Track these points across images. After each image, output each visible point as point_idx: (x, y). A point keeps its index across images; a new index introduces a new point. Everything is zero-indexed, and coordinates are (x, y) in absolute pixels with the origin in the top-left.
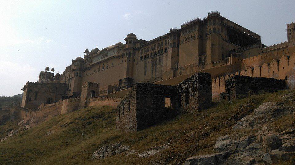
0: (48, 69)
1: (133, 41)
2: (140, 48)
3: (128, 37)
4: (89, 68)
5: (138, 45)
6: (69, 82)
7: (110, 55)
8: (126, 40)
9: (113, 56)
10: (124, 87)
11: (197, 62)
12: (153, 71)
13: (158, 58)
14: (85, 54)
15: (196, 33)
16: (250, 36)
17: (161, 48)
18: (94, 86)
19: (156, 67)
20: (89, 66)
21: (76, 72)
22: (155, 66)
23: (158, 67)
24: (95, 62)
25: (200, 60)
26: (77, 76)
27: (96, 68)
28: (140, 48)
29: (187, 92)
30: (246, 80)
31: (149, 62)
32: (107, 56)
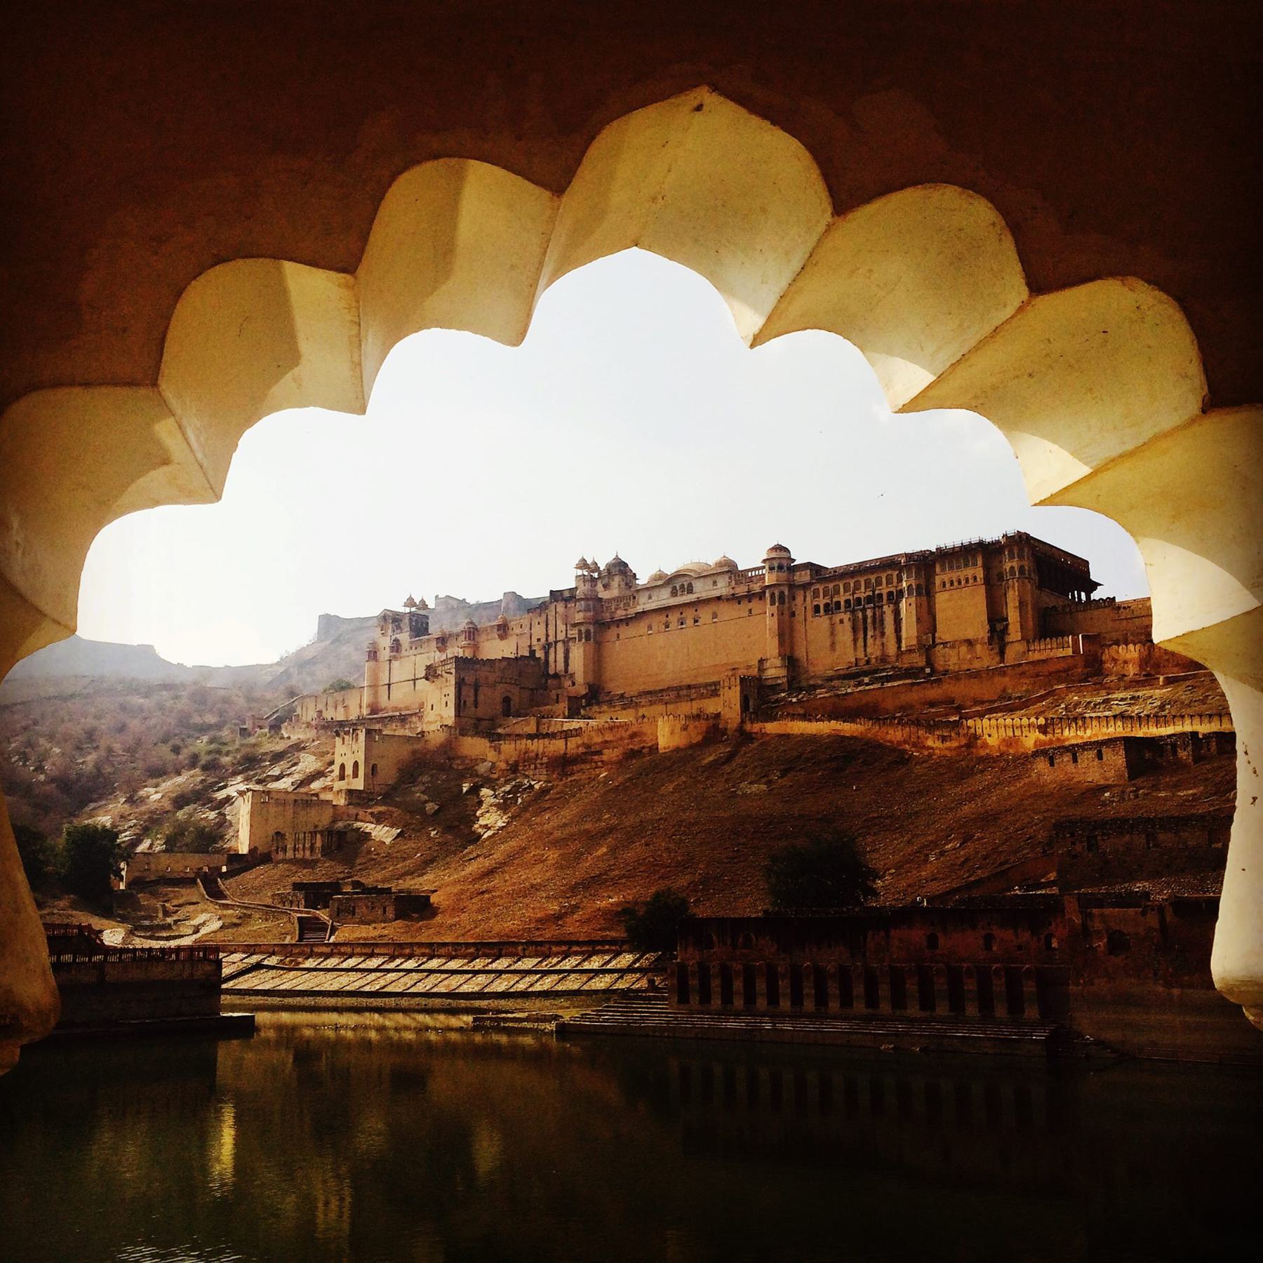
0: (410, 602)
2: (810, 584)
4: (627, 621)
5: (804, 577)
7: (702, 590)
8: (764, 561)
9: (716, 593)
12: (855, 641)
14: (580, 572)
15: (980, 573)
20: (620, 614)
23: (870, 633)
24: (644, 604)
25: (992, 630)
26: (588, 638)
27: (658, 621)
28: (810, 584)
29: (1174, 746)
31: (842, 621)
32: (690, 591)
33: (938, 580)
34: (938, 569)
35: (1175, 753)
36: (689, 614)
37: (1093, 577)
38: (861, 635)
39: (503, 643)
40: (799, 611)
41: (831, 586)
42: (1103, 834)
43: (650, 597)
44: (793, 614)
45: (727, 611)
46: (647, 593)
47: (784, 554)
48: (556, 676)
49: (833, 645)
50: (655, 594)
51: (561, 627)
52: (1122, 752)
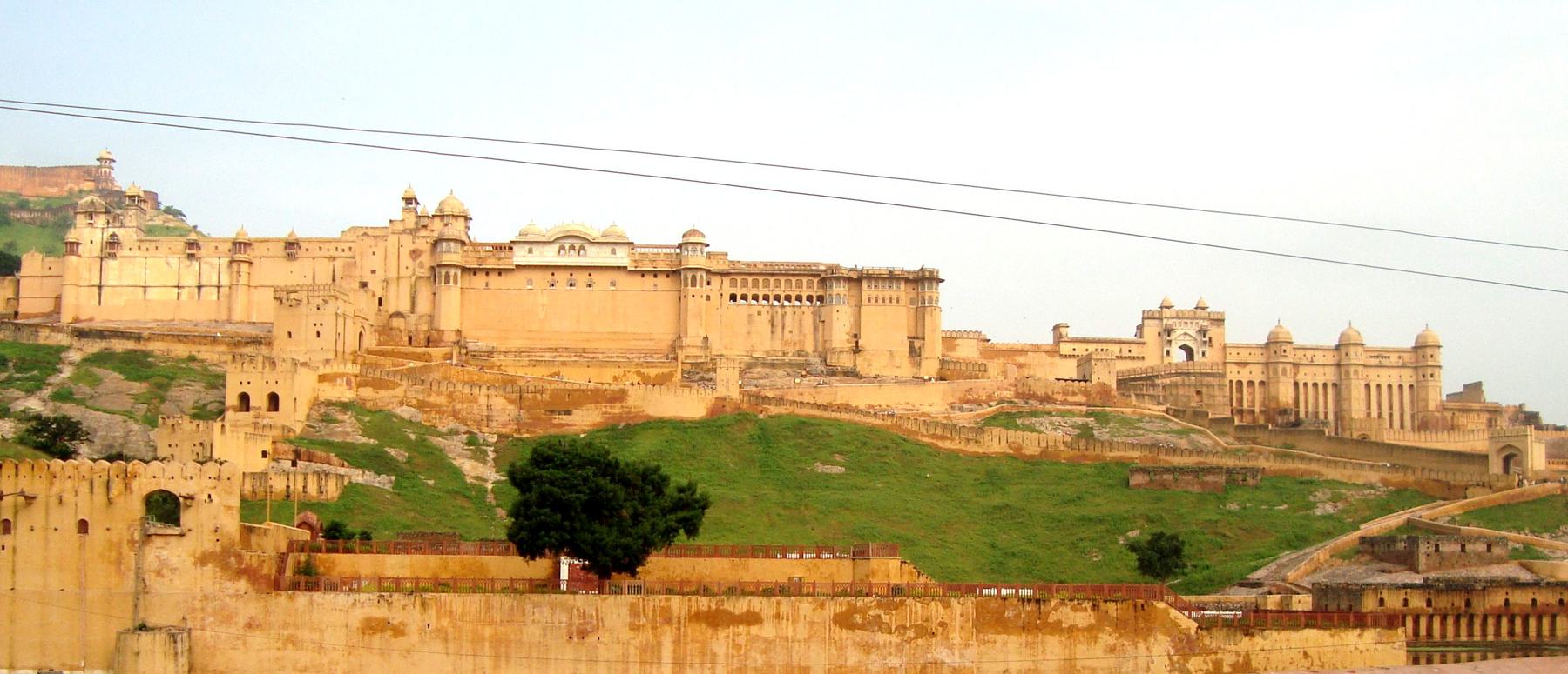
4: (500, 272)
6: (385, 289)
7: (596, 256)
21: (452, 272)
25: (911, 347)
27: (541, 279)
33: (865, 295)
34: (865, 284)
36: (582, 278)
38: (779, 329)
39: (295, 265)
40: (715, 296)
43: (530, 251)
44: (708, 298)
45: (623, 280)
46: (527, 247)
48: (398, 315)
50: (537, 249)
51: (406, 260)
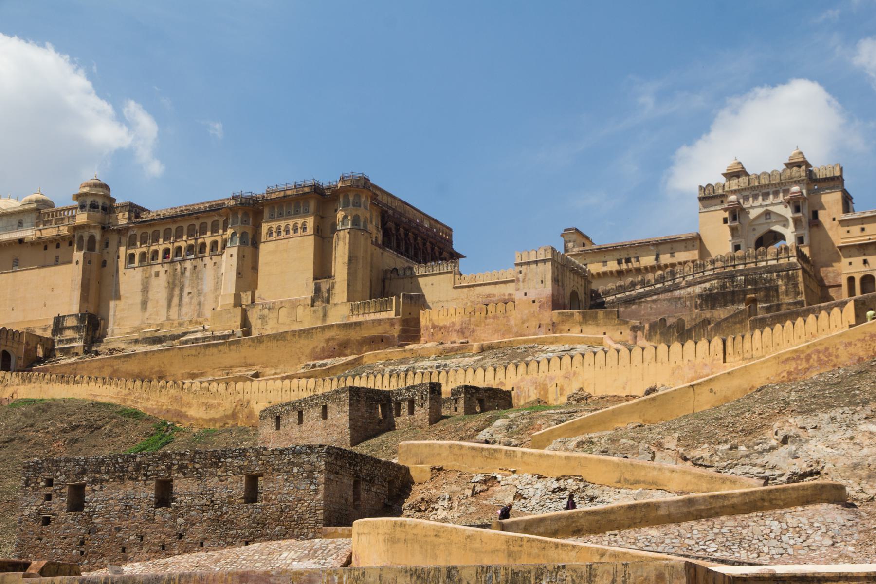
1: (100, 204)
3: (87, 190)
10: (72, 340)
11: (309, 294)
13: (188, 265)
15: (310, 222)
16: (430, 229)
17: (200, 241)
18: (10, 337)
19: (182, 290)
22: (177, 292)
23: (187, 290)
25: (318, 290)
29: (412, 403)
30: (474, 391)
31: (157, 274)
33: (265, 227)
35: (411, 411)
37: (457, 247)
41: (150, 231)
42: (94, 481)
44: (104, 264)
47: (100, 191)
49: (144, 304)
52: (347, 408)
